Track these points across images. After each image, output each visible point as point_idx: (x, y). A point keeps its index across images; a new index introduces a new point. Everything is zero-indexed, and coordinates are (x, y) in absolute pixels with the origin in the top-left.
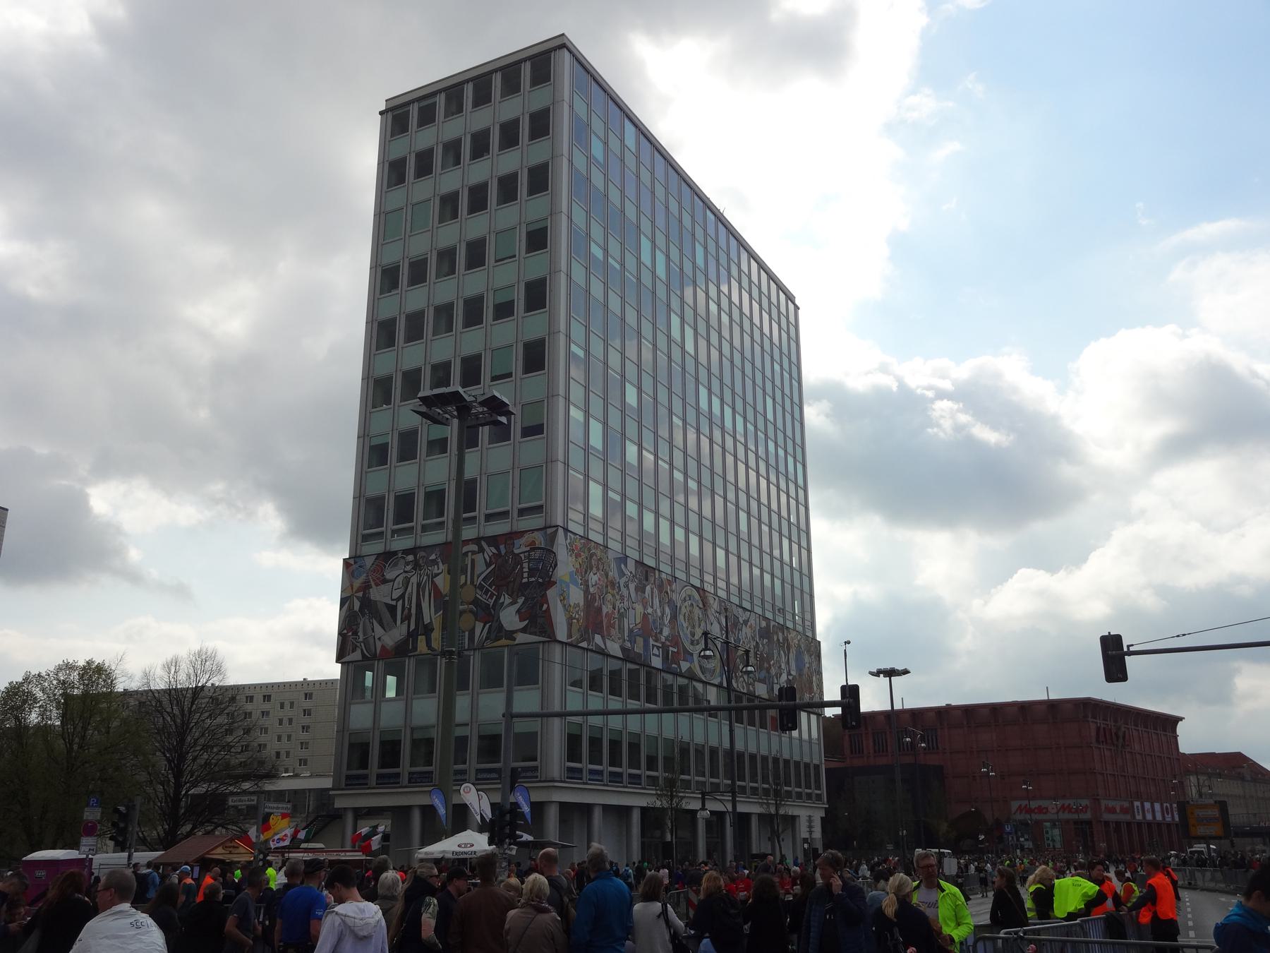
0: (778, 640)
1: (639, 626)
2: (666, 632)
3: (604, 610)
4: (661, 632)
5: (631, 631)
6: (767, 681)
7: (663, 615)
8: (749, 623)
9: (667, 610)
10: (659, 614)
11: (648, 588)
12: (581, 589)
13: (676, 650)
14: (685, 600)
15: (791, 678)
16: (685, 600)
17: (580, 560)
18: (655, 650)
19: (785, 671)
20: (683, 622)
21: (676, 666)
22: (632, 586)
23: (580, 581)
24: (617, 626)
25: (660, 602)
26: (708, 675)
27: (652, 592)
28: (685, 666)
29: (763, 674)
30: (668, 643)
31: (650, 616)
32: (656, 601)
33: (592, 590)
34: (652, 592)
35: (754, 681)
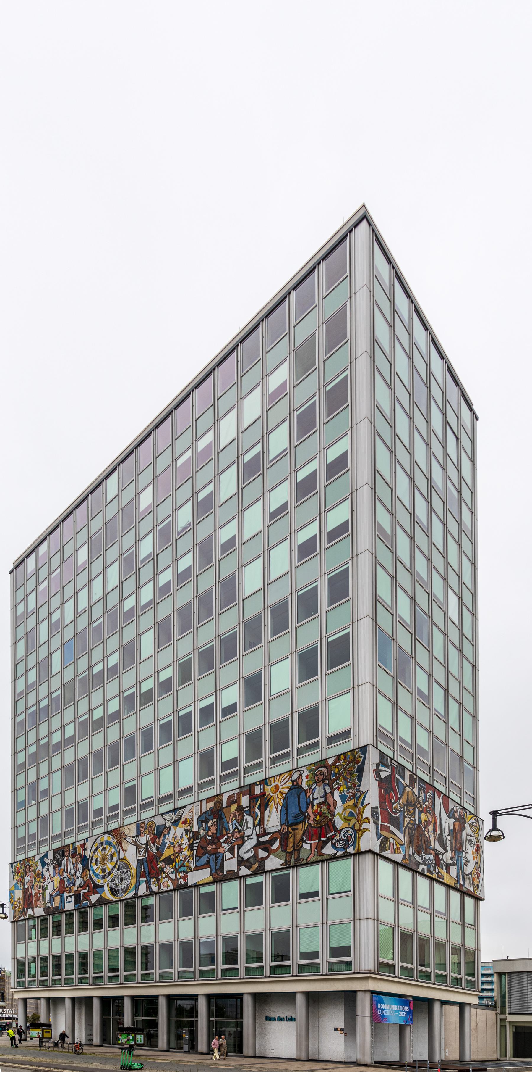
0: (240, 808)
1: (57, 889)
2: (78, 882)
3: (34, 892)
4: (74, 885)
5: (51, 896)
6: (212, 864)
7: (76, 873)
8: (183, 820)
9: (80, 866)
10: (73, 872)
11: (64, 862)
12: (20, 889)
13: (86, 891)
14: (97, 849)
15: (266, 838)
16: (97, 849)
17: (20, 874)
18: (69, 899)
19: (254, 836)
20: (95, 867)
21: (87, 901)
22: (51, 868)
23: (20, 886)
24: (41, 898)
25: (73, 864)
26: (120, 895)
27: (67, 862)
28: (94, 898)
29: (204, 859)
30: (80, 889)
31: (65, 879)
32: (71, 866)
33: (26, 886)
34: (67, 862)
35: (187, 873)
